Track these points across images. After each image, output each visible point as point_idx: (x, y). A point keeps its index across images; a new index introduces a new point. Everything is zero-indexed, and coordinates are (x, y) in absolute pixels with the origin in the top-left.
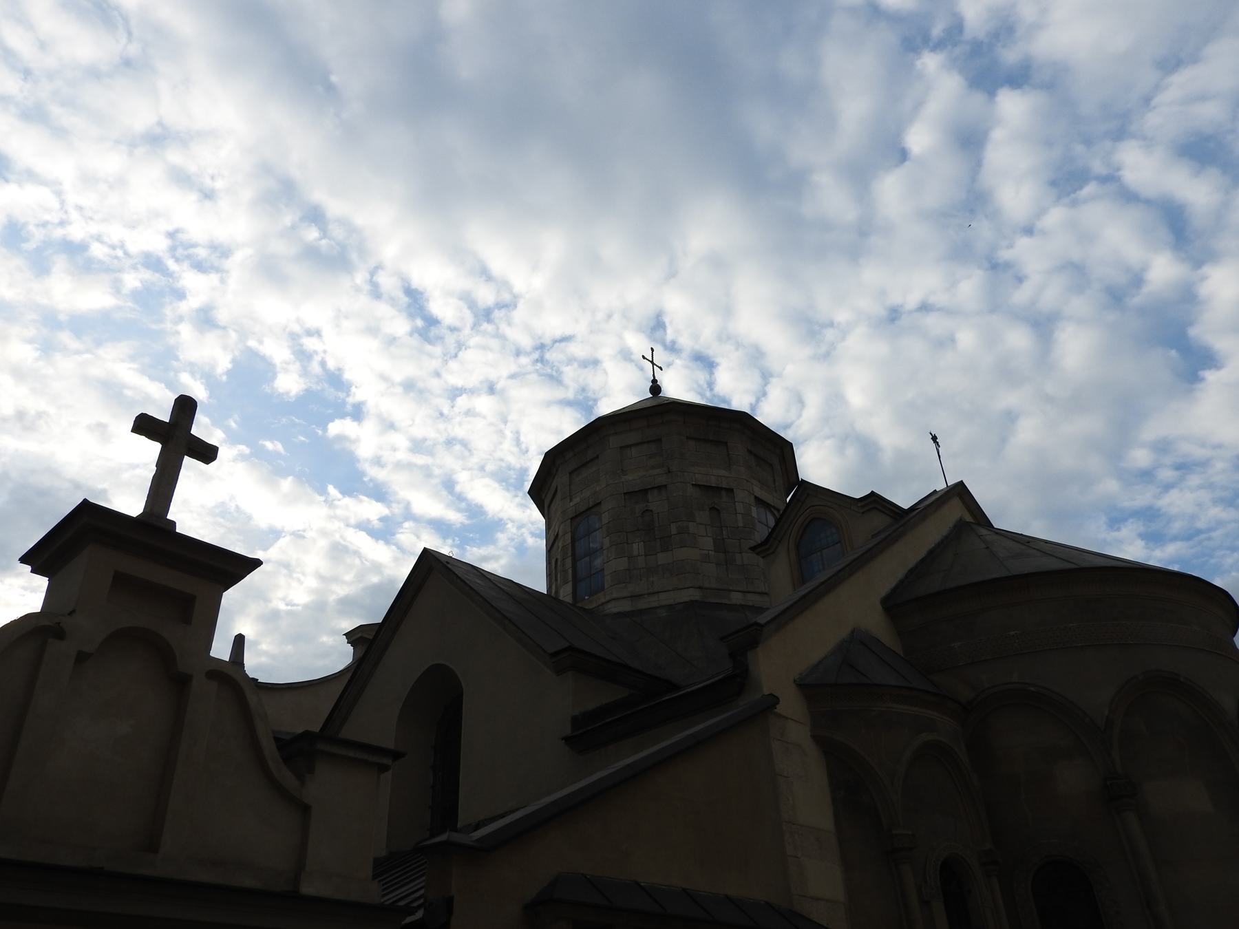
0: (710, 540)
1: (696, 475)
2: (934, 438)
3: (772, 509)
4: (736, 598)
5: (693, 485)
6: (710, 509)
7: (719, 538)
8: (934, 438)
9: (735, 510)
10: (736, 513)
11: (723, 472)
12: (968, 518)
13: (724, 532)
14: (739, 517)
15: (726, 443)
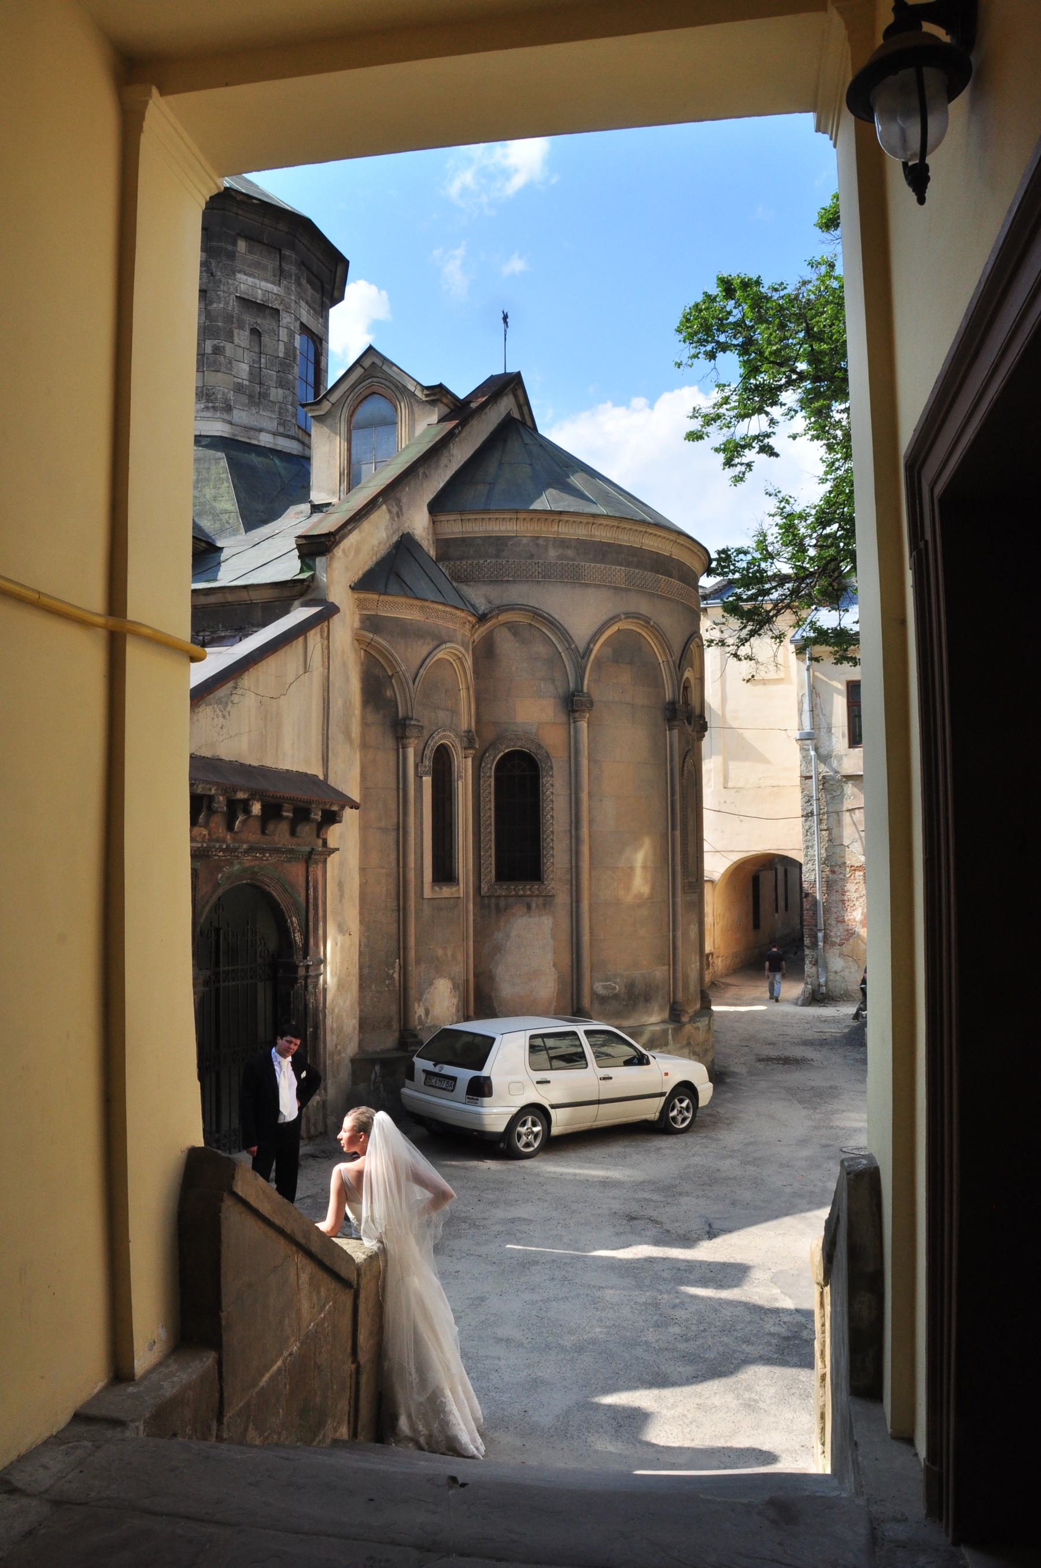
0: (245, 367)
1: (242, 285)
2: (505, 318)
3: (315, 338)
4: (265, 440)
5: (236, 296)
6: (251, 330)
7: (256, 366)
8: (505, 318)
9: (279, 336)
10: (279, 340)
11: (270, 286)
12: (516, 415)
13: (263, 360)
14: (281, 345)
15: (280, 251)
